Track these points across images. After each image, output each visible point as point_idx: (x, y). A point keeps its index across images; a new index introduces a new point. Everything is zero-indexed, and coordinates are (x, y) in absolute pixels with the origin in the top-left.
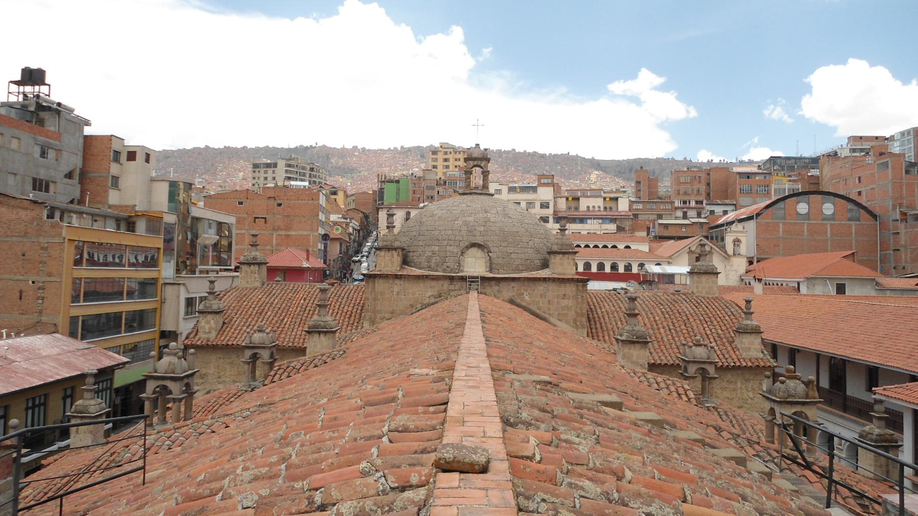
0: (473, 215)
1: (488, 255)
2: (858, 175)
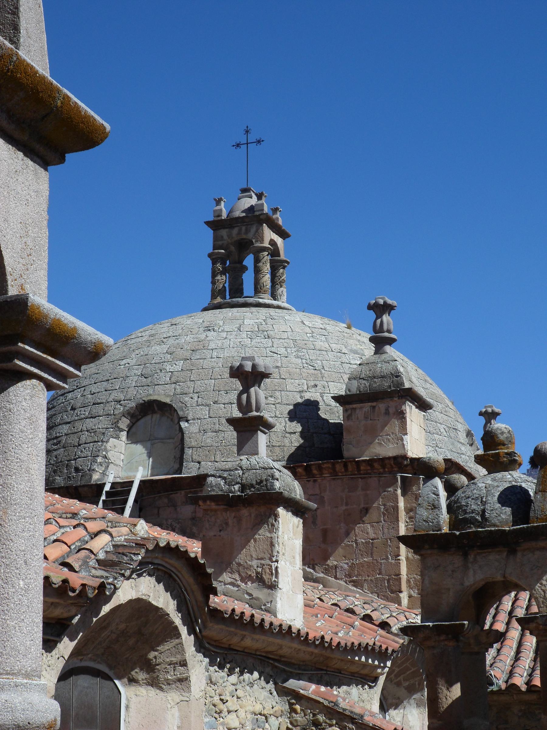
0: (171, 341)
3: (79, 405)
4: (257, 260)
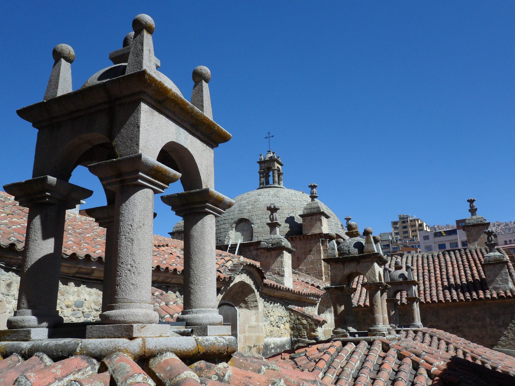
0: (248, 199)
3: (220, 220)
4: (273, 173)
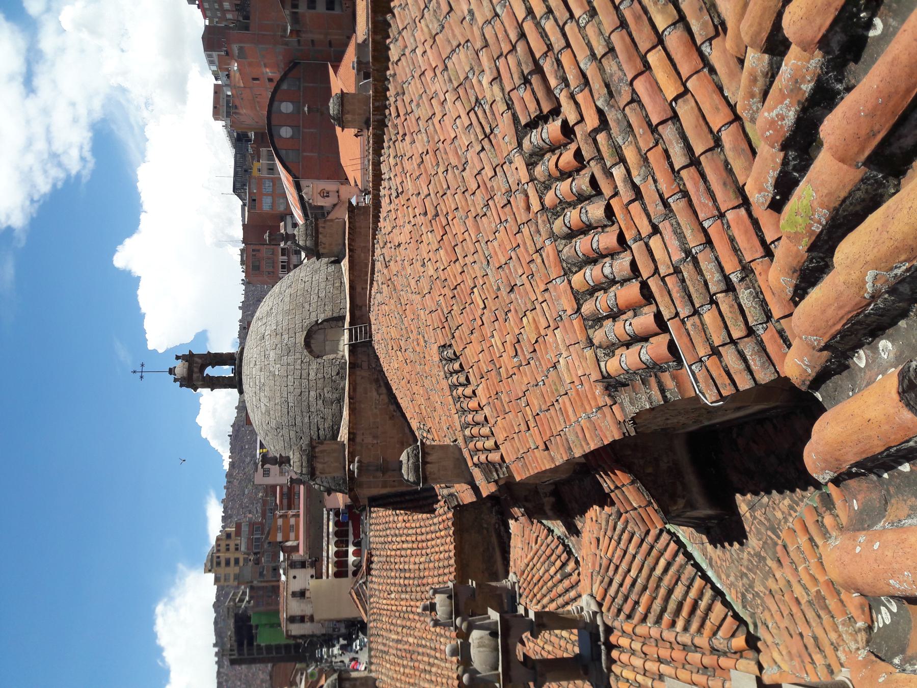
0: (267, 353)
1: (321, 323)
2: (251, 80)
